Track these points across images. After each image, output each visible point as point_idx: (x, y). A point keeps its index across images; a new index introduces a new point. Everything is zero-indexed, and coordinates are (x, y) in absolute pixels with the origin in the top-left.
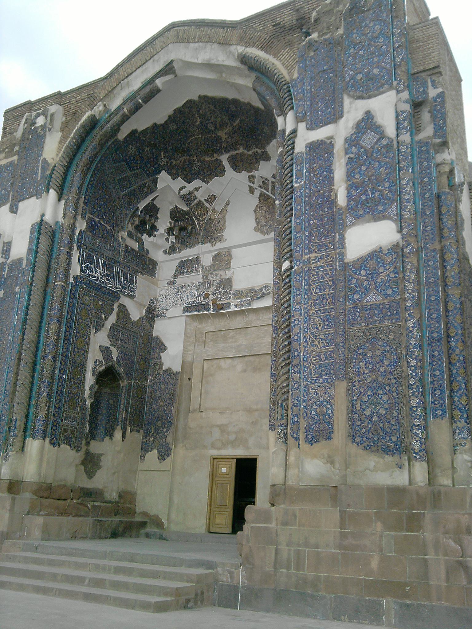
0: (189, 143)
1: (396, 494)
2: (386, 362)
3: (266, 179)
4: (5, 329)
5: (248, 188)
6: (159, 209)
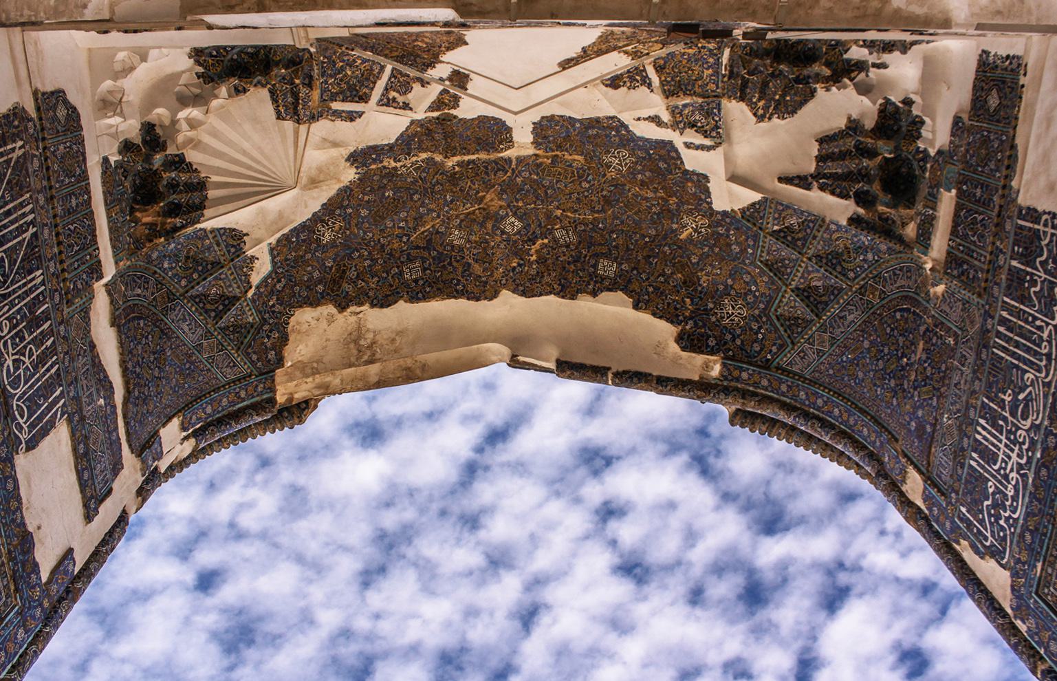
0: (598, 212)
3: (386, 102)
5: (469, 86)
6: (822, 141)
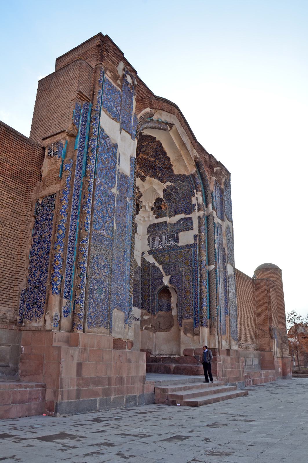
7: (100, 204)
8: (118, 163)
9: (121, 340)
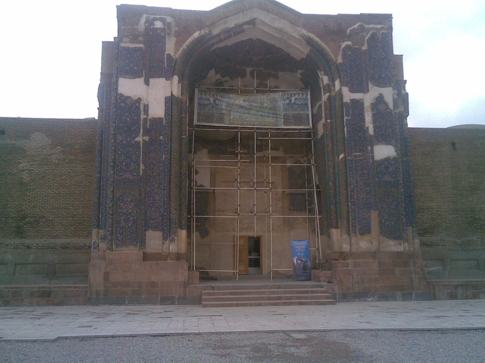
1: (399, 254)
2: (394, 205)
4: (155, 162)
7: (122, 156)
8: (142, 113)
9: (159, 254)
